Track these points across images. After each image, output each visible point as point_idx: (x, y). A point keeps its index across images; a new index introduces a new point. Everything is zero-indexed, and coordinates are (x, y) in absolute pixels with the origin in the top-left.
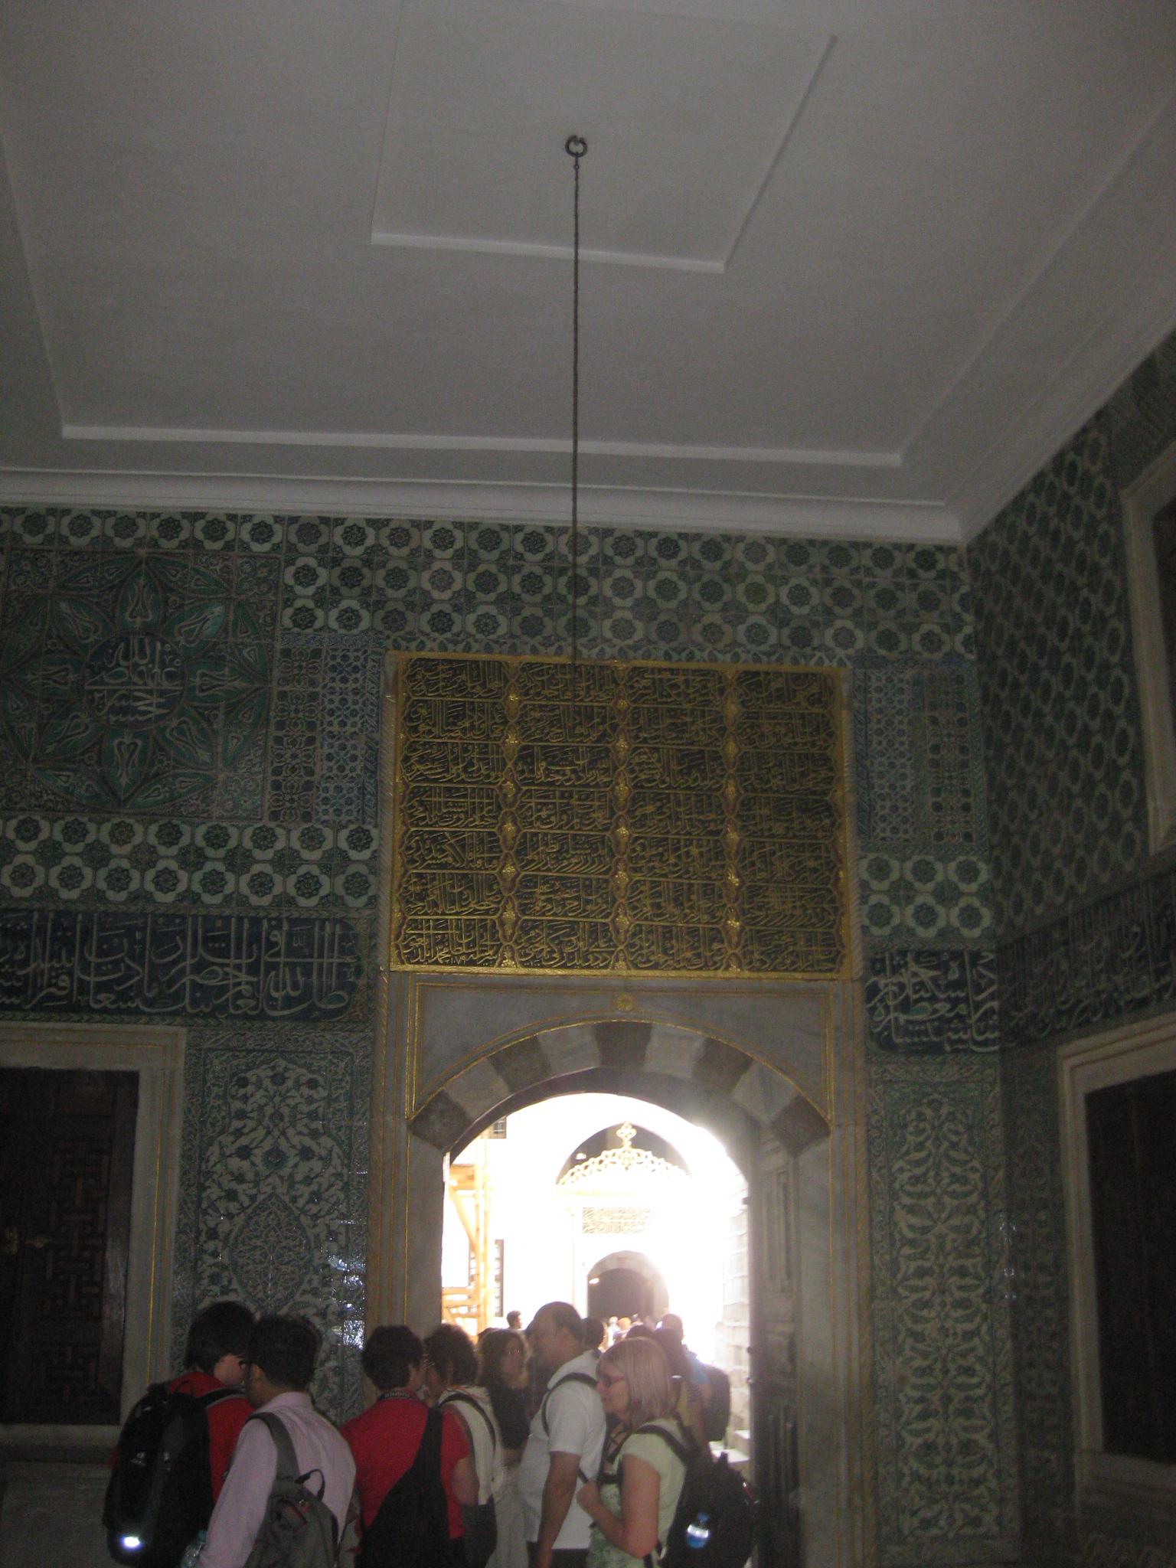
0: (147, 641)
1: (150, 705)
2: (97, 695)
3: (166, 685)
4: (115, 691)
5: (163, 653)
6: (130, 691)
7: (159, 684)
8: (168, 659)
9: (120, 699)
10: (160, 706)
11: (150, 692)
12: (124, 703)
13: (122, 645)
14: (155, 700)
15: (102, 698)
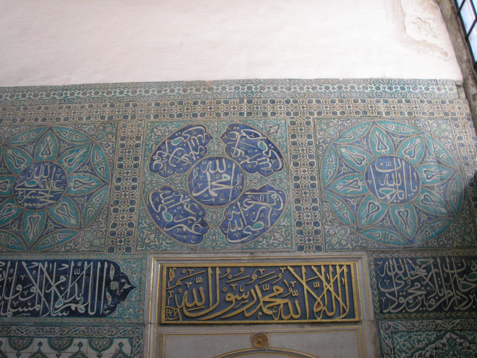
0: (49, 166)
1: (46, 198)
2: (20, 193)
3: (55, 189)
4: (30, 191)
5: (56, 173)
6: (37, 191)
7: (52, 188)
8: (58, 176)
9: (31, 195)
10: (51, 199)
11: (47, 192)
12: (33, 197)
13: (37, 168)
14: (48, 196)
15: (22, 194)
